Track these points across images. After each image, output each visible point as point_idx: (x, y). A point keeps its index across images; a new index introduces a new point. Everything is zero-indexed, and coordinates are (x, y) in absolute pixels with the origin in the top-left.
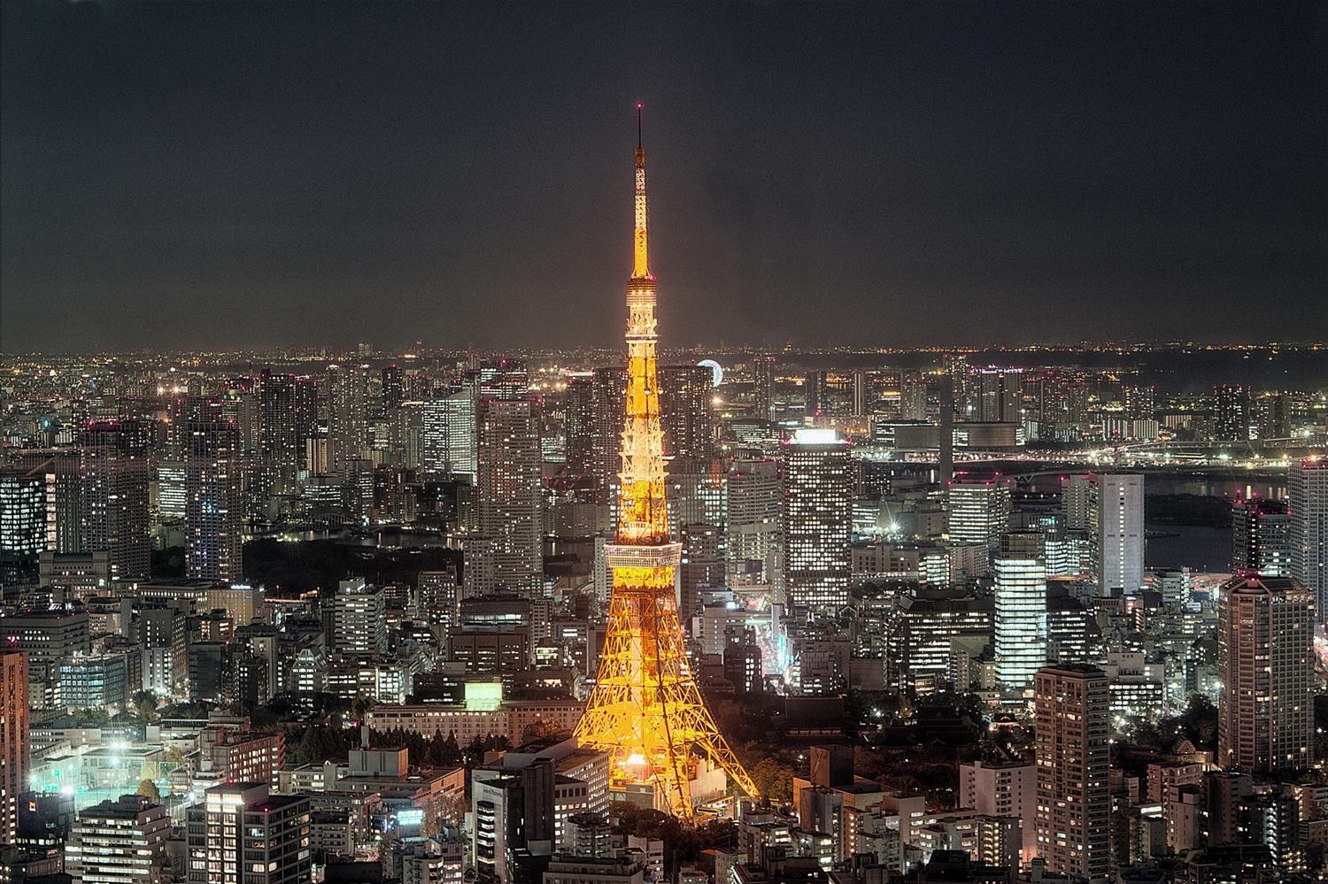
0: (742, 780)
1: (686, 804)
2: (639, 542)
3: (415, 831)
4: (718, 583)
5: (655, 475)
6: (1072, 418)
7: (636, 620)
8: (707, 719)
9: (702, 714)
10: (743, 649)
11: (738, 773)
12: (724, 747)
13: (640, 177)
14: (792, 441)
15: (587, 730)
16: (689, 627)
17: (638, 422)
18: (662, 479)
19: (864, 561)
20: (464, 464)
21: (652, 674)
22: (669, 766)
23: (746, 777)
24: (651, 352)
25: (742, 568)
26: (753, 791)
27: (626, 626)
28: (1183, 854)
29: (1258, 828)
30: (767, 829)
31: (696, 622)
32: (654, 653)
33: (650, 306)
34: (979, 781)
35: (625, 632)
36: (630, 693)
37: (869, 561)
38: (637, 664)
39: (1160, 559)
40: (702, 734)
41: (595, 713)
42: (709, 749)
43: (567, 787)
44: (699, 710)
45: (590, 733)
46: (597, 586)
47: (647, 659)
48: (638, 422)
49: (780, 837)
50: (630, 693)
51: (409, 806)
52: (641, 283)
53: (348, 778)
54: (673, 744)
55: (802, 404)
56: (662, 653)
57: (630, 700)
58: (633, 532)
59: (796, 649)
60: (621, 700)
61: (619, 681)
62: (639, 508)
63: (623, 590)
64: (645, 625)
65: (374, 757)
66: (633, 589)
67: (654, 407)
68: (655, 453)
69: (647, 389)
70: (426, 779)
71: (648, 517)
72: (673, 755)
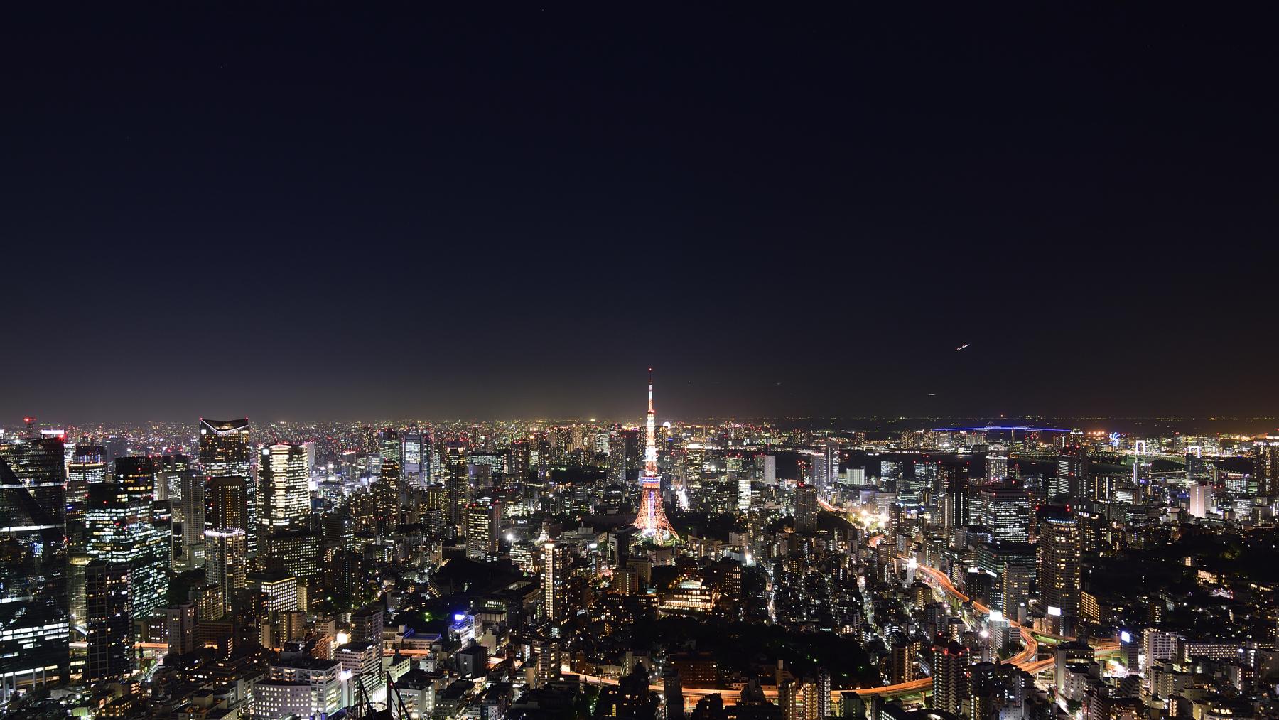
2: (650, 476)
3: (594, 549)
4: (669, 482)
6: (757, 438)
10: (675, 499)
13: (650, 386)
17: (650, 447)
20: (606, 450)
24: (653, 430)
26: (678, 538)
28: (784, 555)
29: (802, 547)
30: (682, 549)
33: (653, 418)
34: (734, 536)
39: (781, 475)
41: (639, 519)
42: (667, 527)
48: (650, 447)
51: (593, 542)
52: (650, 413)
53: (578, 534)
59: (689, 500)
61: (645, 511)
65: (585, 529)
67: (654, 443)
70: (598, 535)
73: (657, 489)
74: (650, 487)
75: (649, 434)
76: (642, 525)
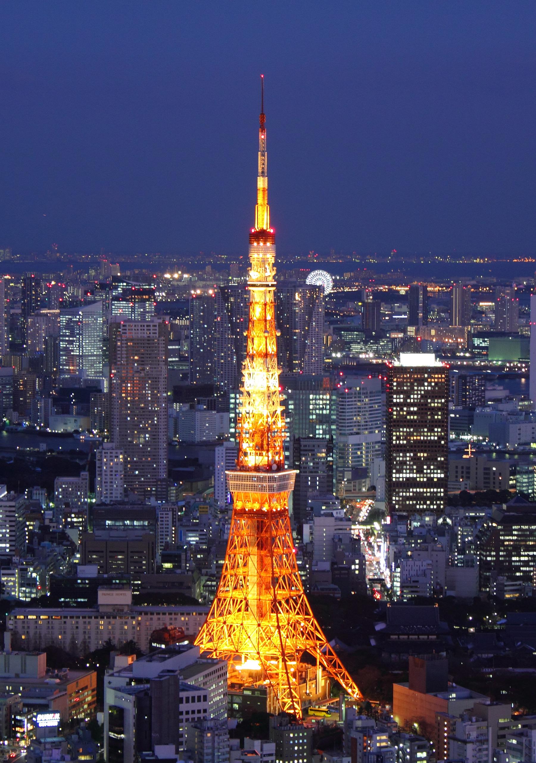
0: (347, 685)
1: (296, 706)
2: (257, 469)
5: (272, 409)
7: (253, 539)
8: (316, 629)
9: (312, 625)
11: (343, 678)
12: (330, 654)
14: (396, 364)
15: (208, 638)
16: (300, 532)
17: (258, 361)
18: (279, 413)
19: (460, 470)
21: (268, 588)
22: (281, 670)
23: (350, 681)
24: (270, 298)
25: (348, 475)
26: (354, 693)
27: (243, 545)
31: (306, 528)
32: (270, 569)
33: (271, 258)
35: (243, 550)
36: (247, 605)
37: (464, 470)
38: (253, 579)
40: (311, 642)
42: (318, 655)
43: (190, 694)
44: (308, 620)
45: (211, 640)
46: (216, 490)
47: (263, 574)
48: (258, 361)
49: (381, 741)
50: (247, 605)
54: (286, 652)
55: (405, 314)
56: (277, 570)
57: (247, 610)
58: (251, 460)
60: (239, 610)
61: (238, 595)
62: (257, 439)
63: (242, 513)
64: (261, 545)
66: (251, 511)
67: (272, 348)
68: (272, 389)
69: (266, 331)
71: (265, 446)
72: (284, 661)
73: (282, 513)
74: (256, 506)
75: (256, 312)
76: (225, 646)
